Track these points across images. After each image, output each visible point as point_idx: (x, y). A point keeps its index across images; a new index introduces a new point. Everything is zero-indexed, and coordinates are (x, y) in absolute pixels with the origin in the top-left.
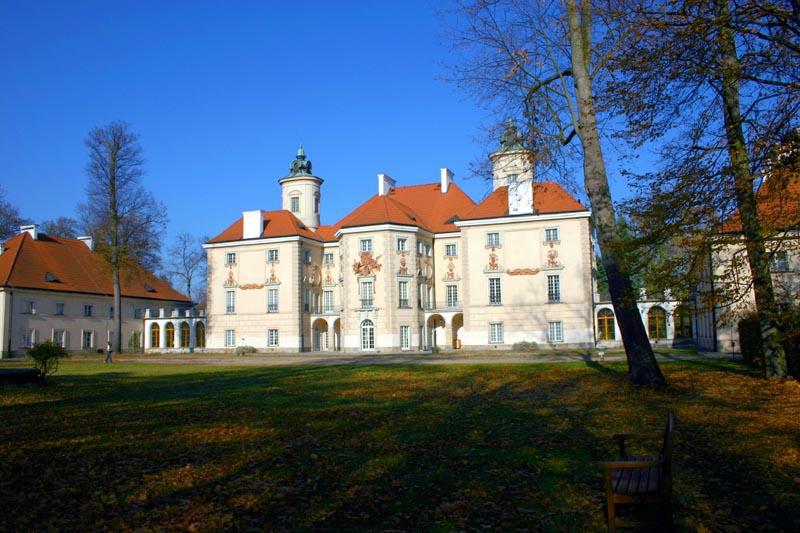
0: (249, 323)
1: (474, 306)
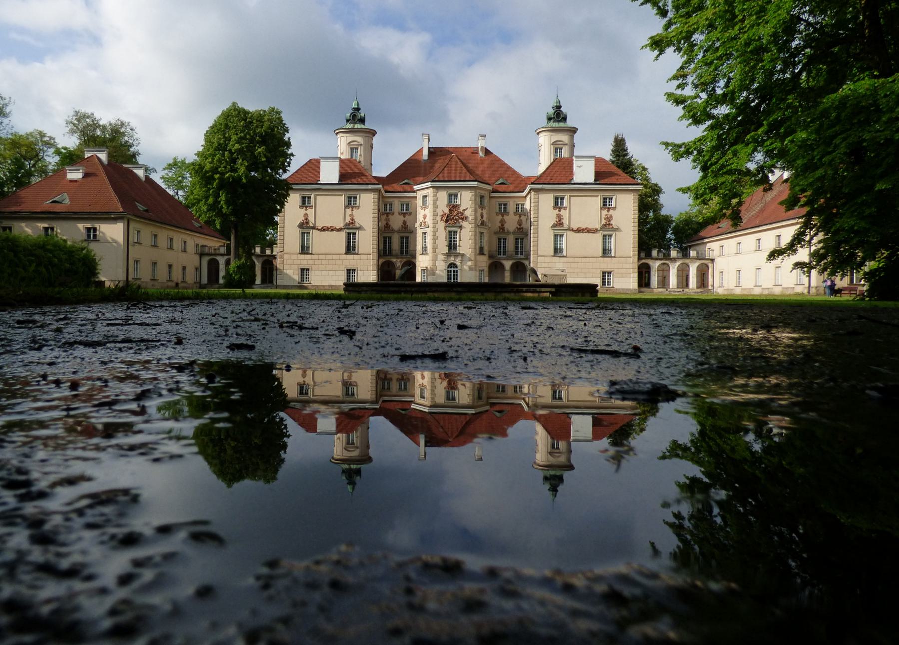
0: (324, 262)
1: (542, 256)
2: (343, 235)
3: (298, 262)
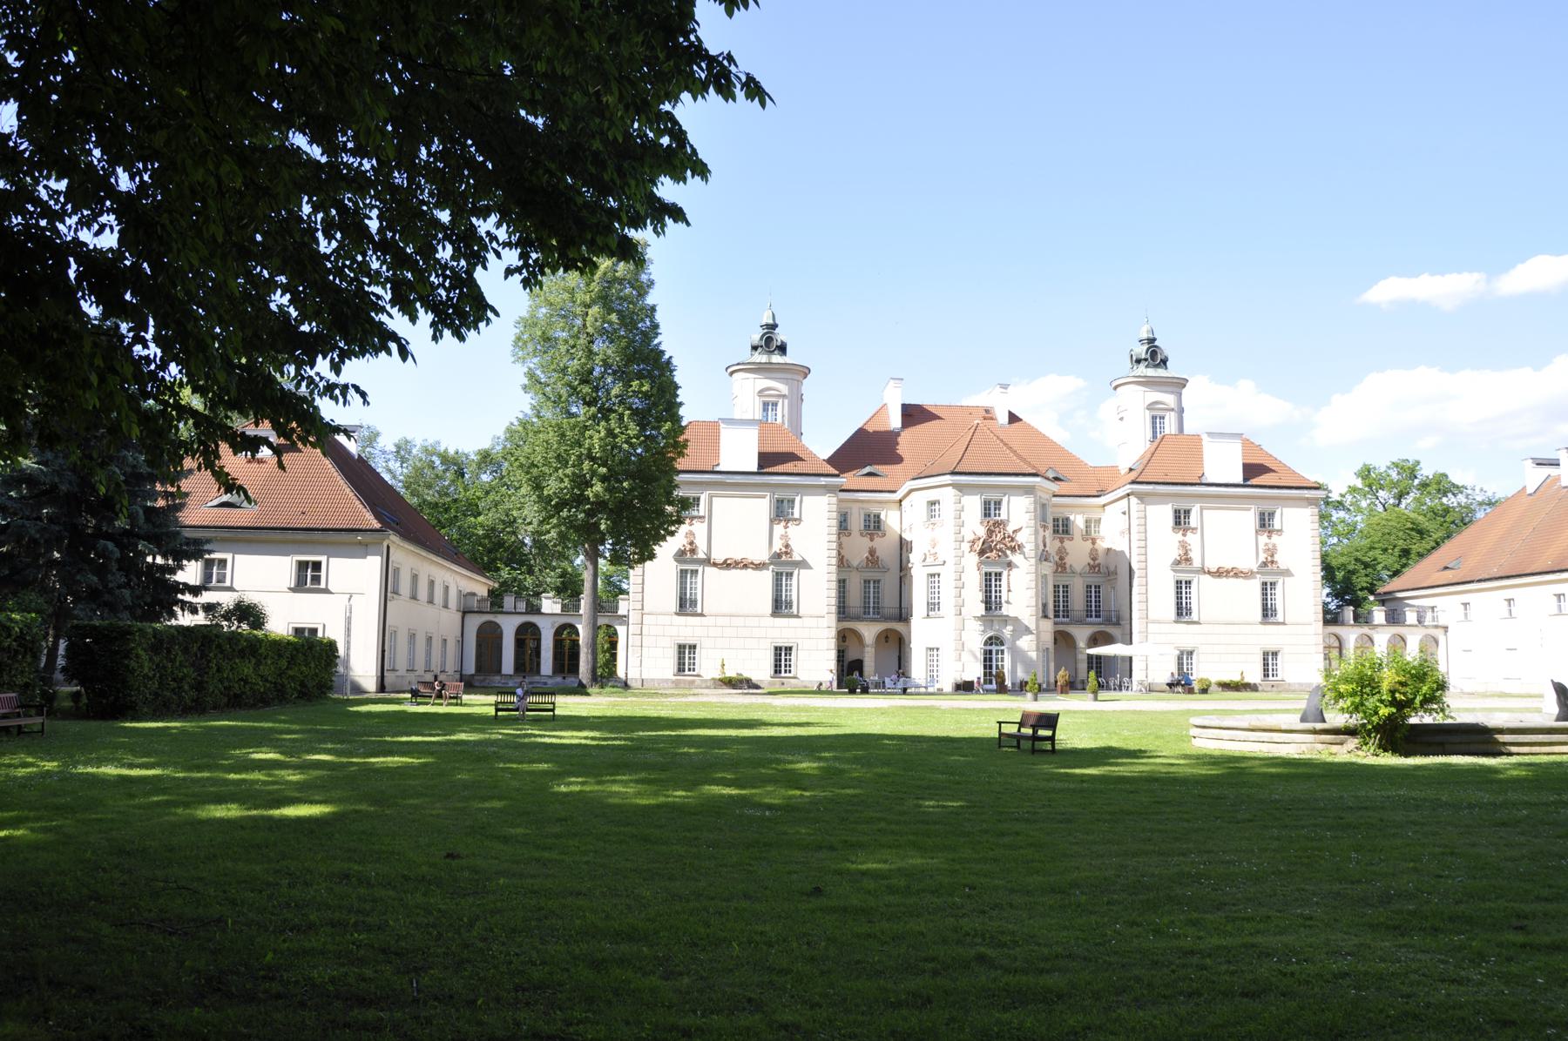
1: (1154, 622)
2: (767, 577)
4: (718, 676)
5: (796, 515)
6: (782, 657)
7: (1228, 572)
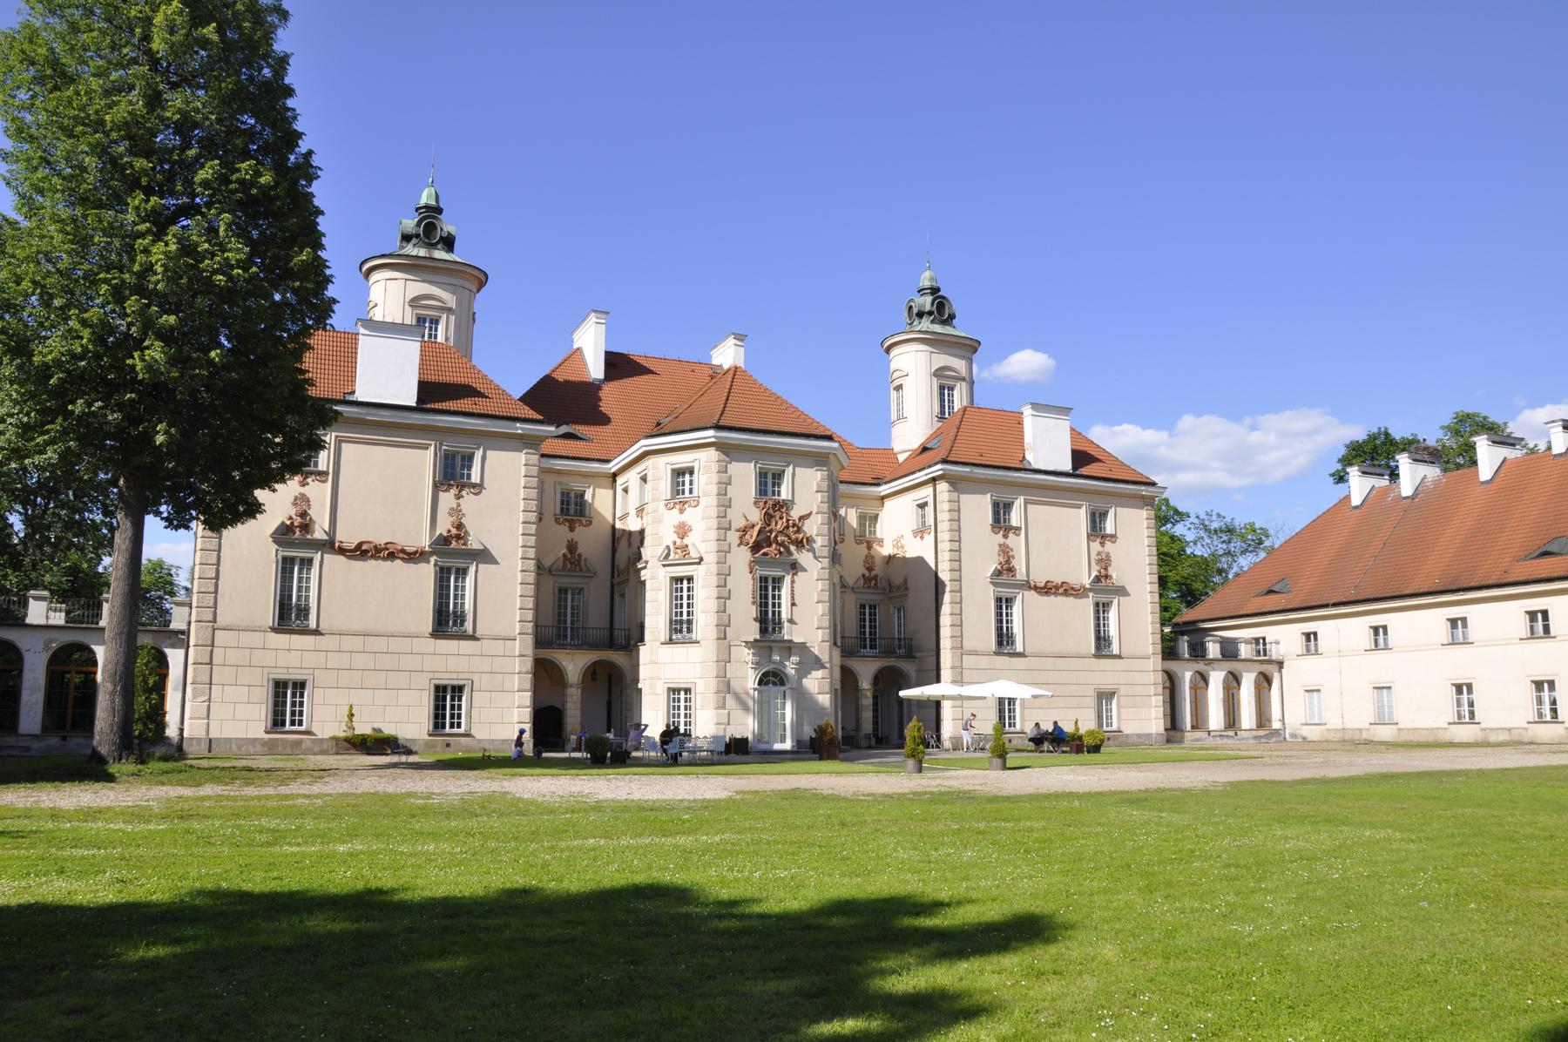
0: (360, 661)
2: (426, 573)
3: (268, 658)
4: (340, 731)
5: (475, 478)
6: (446, 699)
7: (1057, 587)
